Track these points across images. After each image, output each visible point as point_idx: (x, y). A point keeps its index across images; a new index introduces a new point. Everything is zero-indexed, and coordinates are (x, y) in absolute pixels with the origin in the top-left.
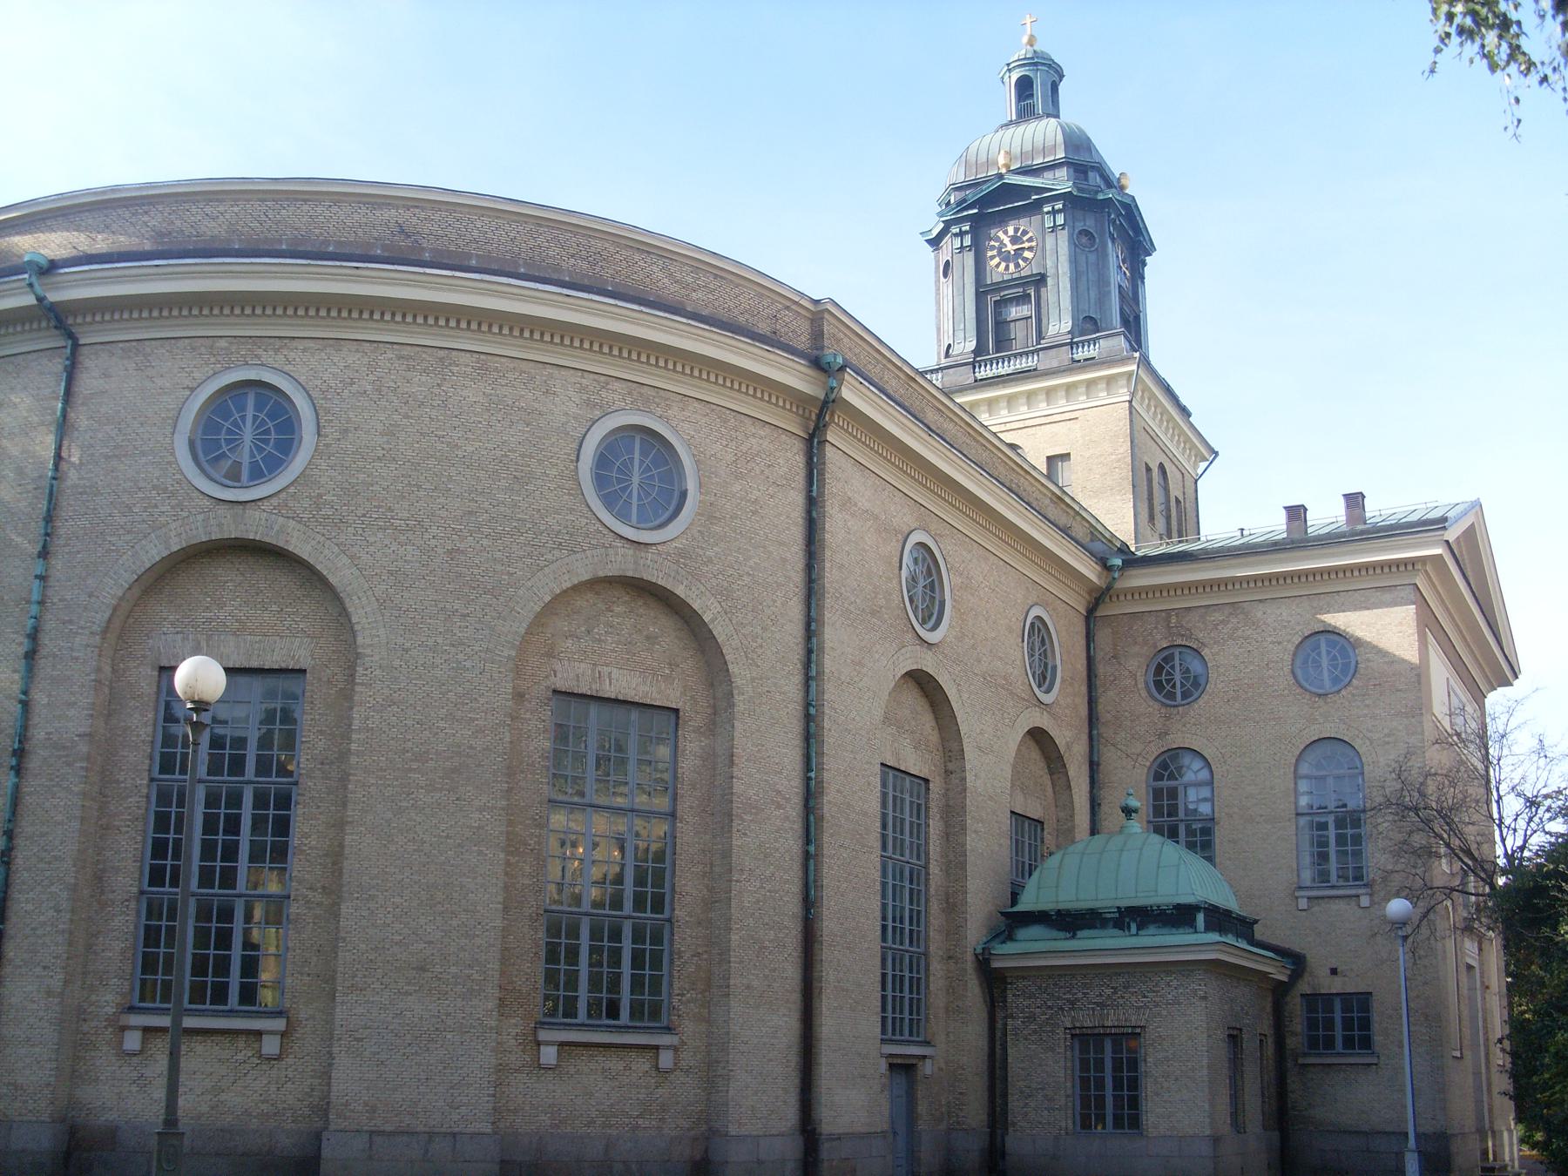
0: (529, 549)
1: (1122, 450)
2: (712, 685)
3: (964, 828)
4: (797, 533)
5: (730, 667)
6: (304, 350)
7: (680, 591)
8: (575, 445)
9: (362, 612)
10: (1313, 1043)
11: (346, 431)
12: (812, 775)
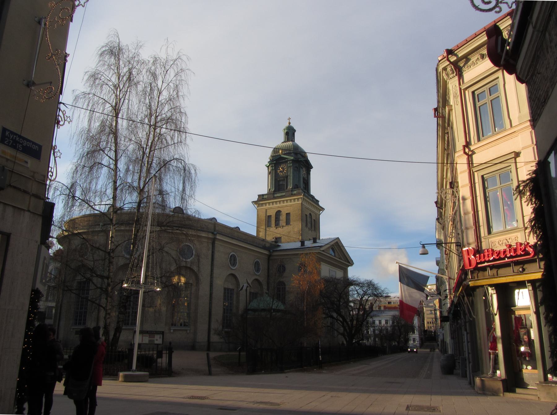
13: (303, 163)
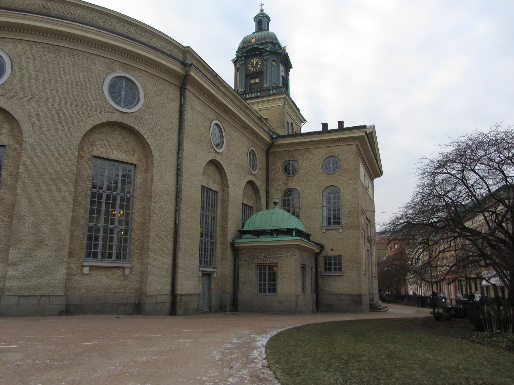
0: (85, 111)
1: (281, 118)
2: (147, 158)
3: (228, 206)
4: (176, 115)
5: (153, 152)
6: (8, 42)
7: (137, 128)
8: (102, 80)
9: (25, 127)
10: (326, 270)
11: (22, 69)
12: (179, 186)
13: (283, 57)
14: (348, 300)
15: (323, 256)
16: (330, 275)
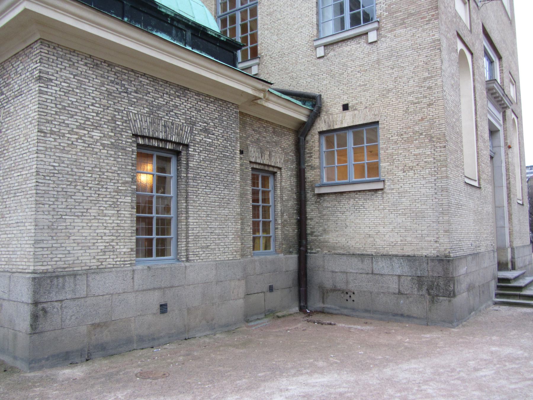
14: (399, 276)
15: (321, 133)
16: (342, 193)
